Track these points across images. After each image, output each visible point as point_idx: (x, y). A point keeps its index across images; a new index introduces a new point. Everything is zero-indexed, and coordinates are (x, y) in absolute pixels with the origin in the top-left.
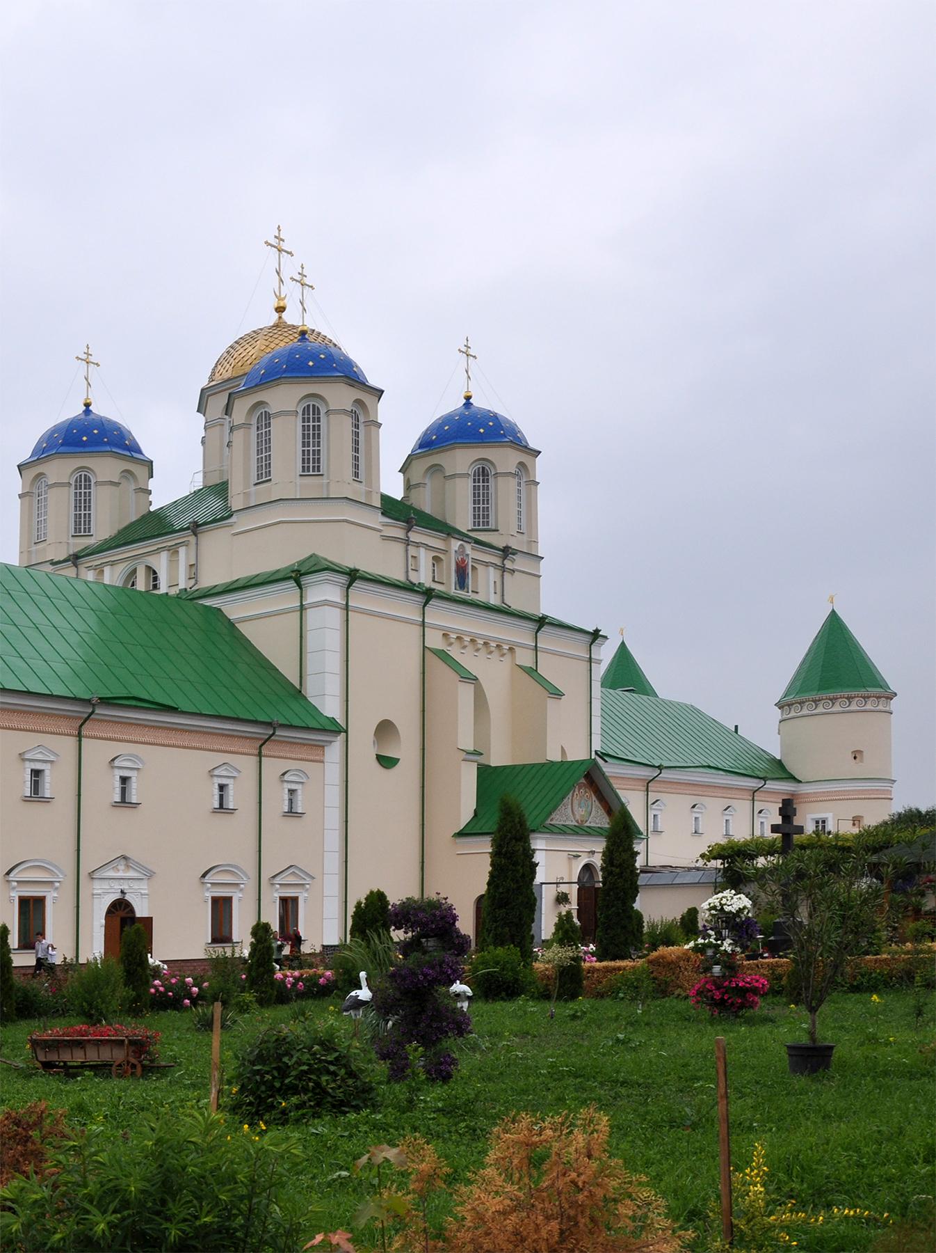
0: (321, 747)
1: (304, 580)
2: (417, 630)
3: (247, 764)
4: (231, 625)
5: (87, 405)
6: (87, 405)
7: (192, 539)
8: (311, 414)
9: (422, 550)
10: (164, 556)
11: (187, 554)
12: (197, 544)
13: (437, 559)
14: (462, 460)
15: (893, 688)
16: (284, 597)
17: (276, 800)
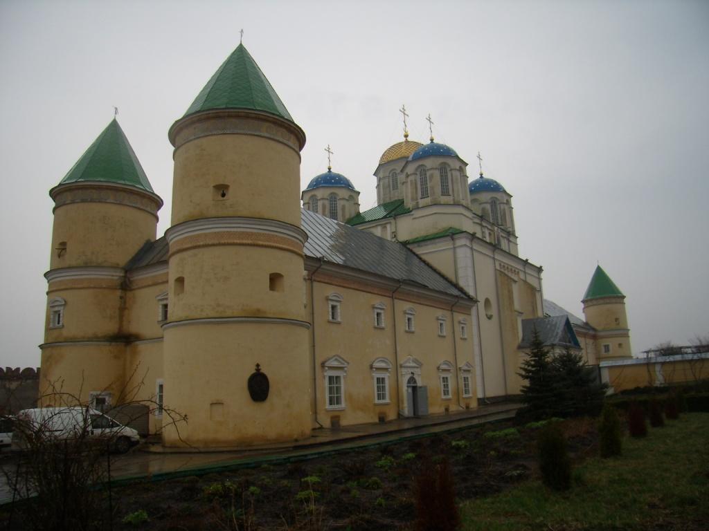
0: (469, 308)
1: (456, 236)
2: (491, 261)
3: (448, 313)
4: (417, 255)
5: (329, 169)
6: (329, 169)
7: (393, 221)
8: (443, 169)
9: (486, 229)
10: (379, 229)
11: (391, 227)
12: (396, 223)
13: (490, 234)
14: (485, 197)
15: (625, 294)
16: (444, 245)
17: (458, 328)
